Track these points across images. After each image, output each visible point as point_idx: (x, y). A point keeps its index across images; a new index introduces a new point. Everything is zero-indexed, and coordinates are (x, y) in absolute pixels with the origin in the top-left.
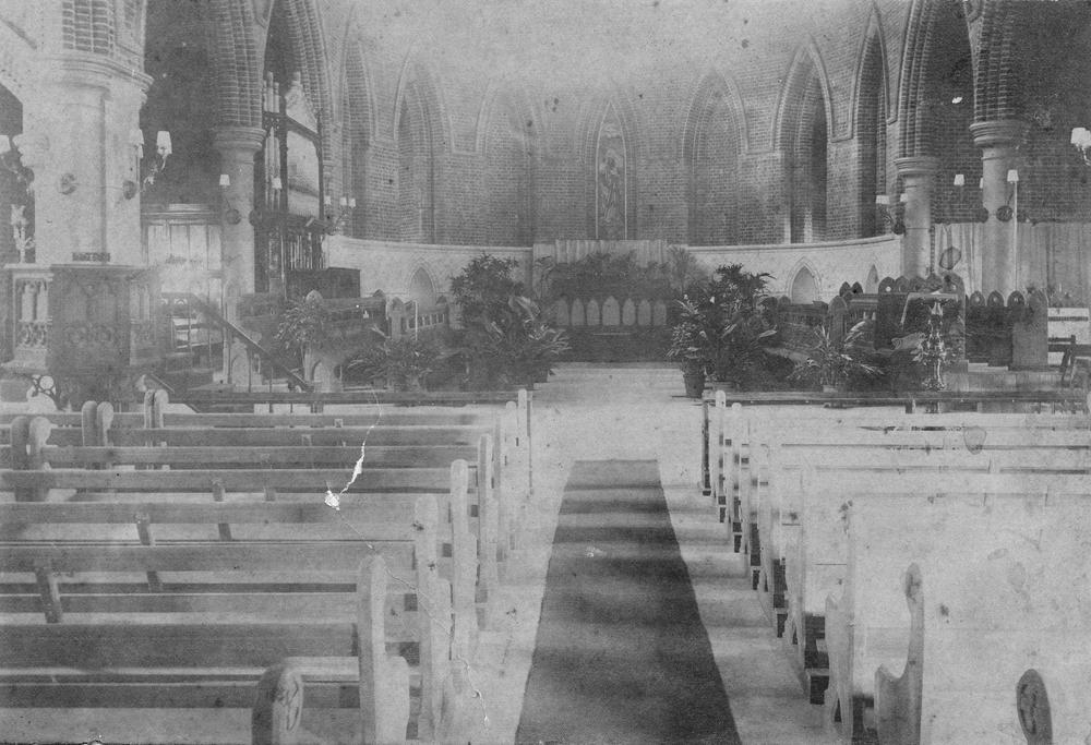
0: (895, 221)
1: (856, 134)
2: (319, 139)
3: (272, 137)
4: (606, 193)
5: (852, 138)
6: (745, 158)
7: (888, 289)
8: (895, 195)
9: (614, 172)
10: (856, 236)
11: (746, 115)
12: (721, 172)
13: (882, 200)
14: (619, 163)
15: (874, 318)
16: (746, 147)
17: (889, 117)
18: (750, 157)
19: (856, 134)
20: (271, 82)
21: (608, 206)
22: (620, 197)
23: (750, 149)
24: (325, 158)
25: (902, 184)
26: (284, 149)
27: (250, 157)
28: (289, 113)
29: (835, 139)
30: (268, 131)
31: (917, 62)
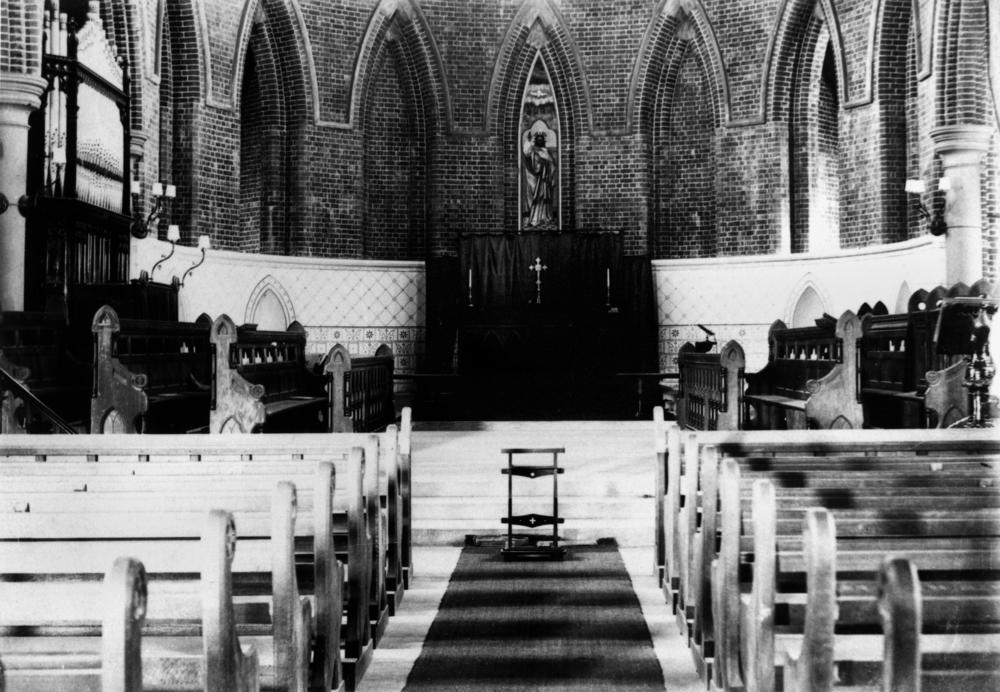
0: (932, 217)
1: (877, 96)
2: (126, 101)
3: (56, 92)
4: (531, 181)
5: (872, 100)
6: (726, 132)
7: (922, 306)
8: (932, 179)
9: (544, 154)
10: (880, 240)
11: (726, 71)
12: (693, 152)
13: (913, 186)
14: (552, 141)
15: (902, 349)
16: (727, 117)
17: (920, 70)
18: (732, 131)
19: (877, 96)
20: (57, 14)
21: (535, 203)
22: (552, 189)
23: (731, 119)
24: (134, 127)
25: (941, 163)
26: (72, 109)
27: (23, 117)
28: (83, 58)
29: (848, 104)
30: (51, 82)
31: (955, 11)
